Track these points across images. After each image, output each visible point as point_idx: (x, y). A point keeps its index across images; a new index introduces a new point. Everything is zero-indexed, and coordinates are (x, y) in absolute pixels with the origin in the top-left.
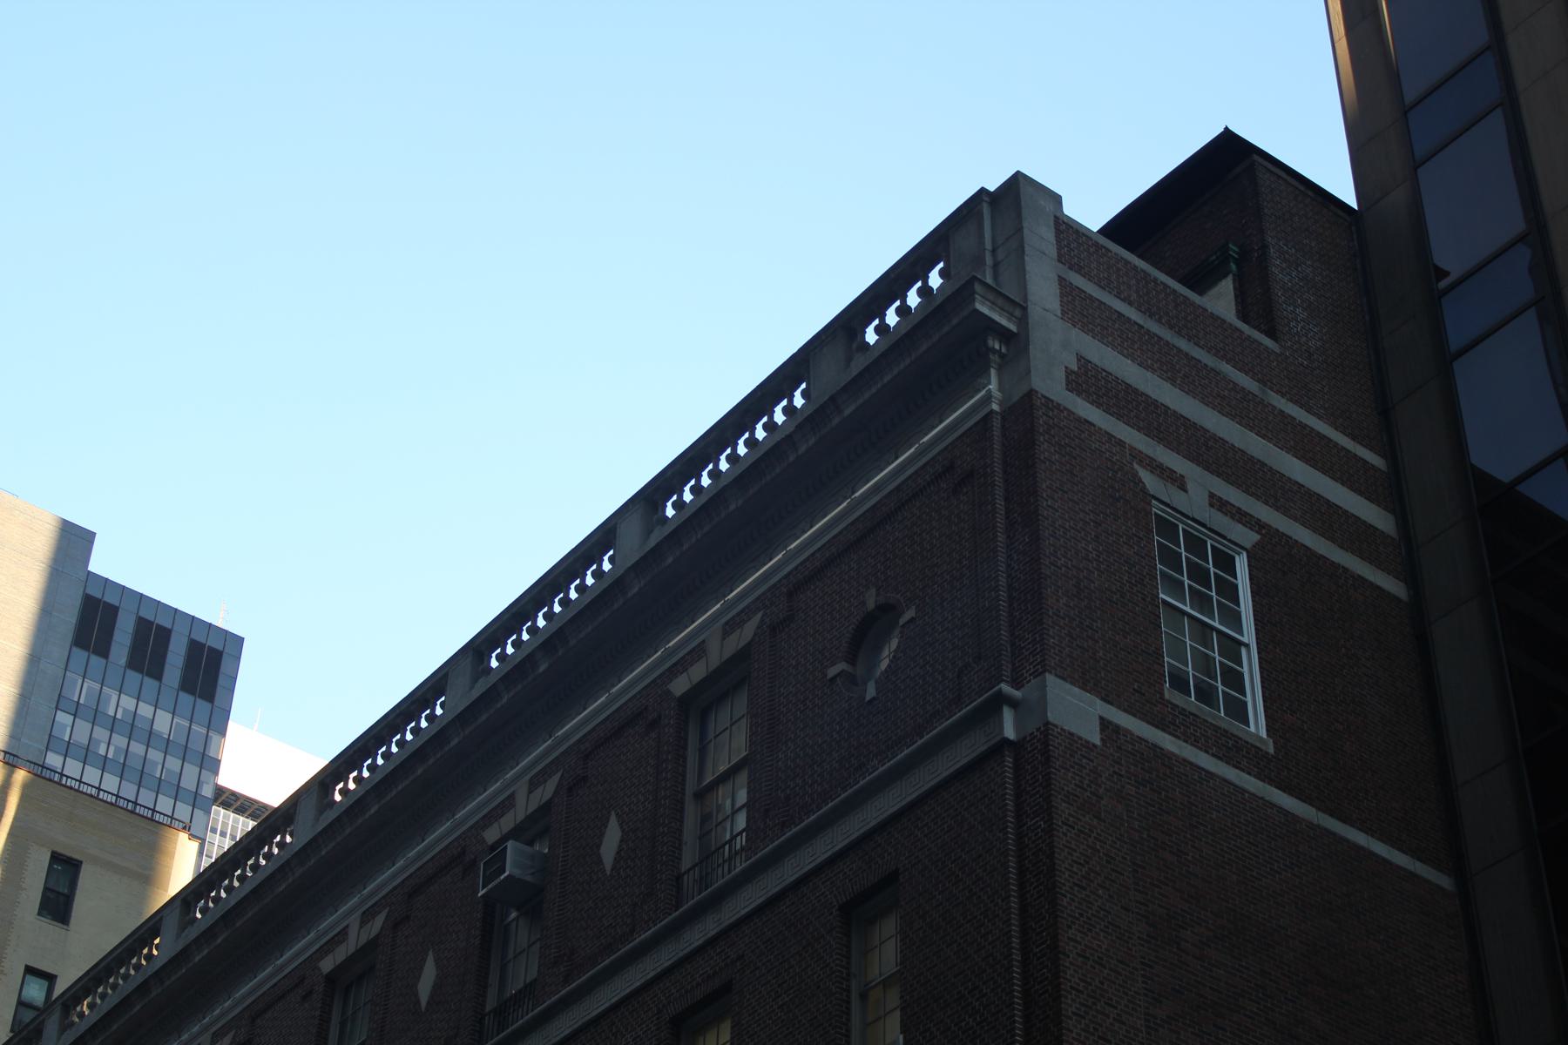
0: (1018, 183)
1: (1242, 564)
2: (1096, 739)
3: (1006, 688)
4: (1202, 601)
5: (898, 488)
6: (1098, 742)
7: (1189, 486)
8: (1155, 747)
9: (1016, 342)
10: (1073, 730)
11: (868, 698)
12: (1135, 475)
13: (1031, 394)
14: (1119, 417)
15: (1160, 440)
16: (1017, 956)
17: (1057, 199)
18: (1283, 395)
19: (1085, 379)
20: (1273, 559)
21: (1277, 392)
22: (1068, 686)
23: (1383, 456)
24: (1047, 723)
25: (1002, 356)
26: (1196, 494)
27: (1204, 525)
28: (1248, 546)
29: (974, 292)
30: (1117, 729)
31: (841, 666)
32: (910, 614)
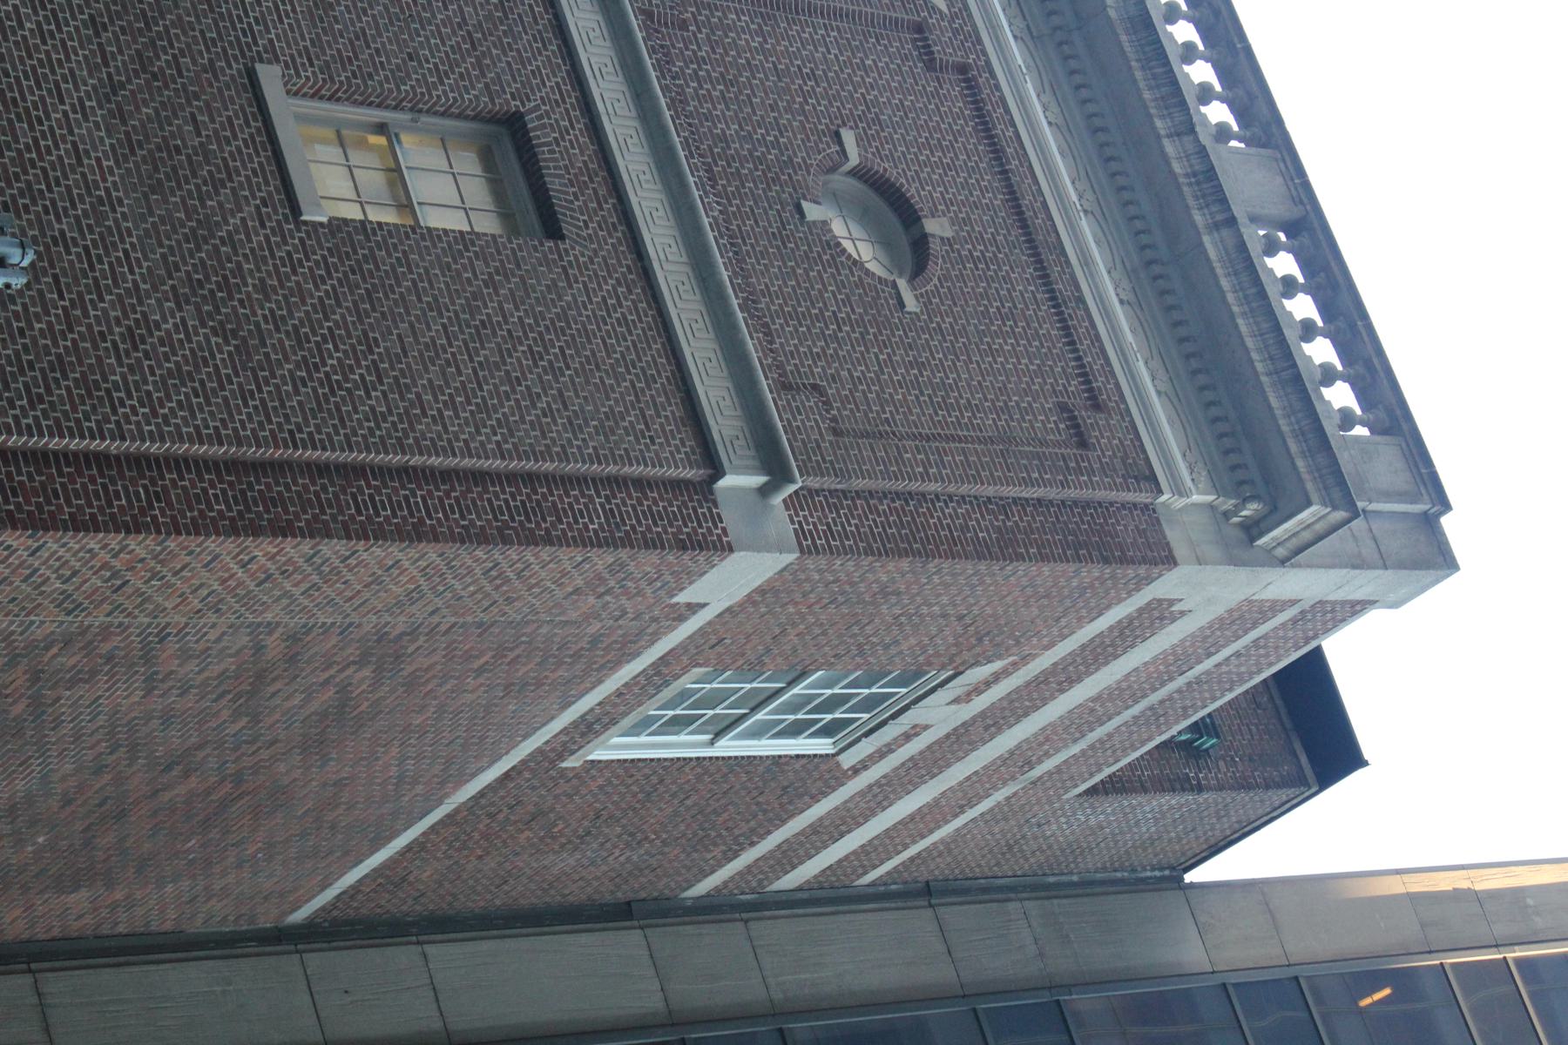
0: (1436, 558)
1: (823, 746)
2: (682, 598)
3: (791, 488)
4: (794, 707)
5: (1081, 300)
6: (675, 600)
7: (953, 707)
8: (636, 655)
9: (1244, 541)
10: (707, 576)
11: (805, 205)
12: (1000, 657)
13: (1170, 561)
14: (1083, 647)
15: (1028, 684)
16: (416, 460)
17: (1396, 605)
18: (1008, 799)
19: (1160, 614)
20: (816, 776)
21: (1015, 794)
22: (769, 574)
23: (873, 884)
24: (731, 550)
25: (1226, 515)
26: (940, 714)
27: (893, 717)
28: (840, 758)
29: (1335, 508)
30: (681, 619)
31: (854, 159)
32: (911, 304)
